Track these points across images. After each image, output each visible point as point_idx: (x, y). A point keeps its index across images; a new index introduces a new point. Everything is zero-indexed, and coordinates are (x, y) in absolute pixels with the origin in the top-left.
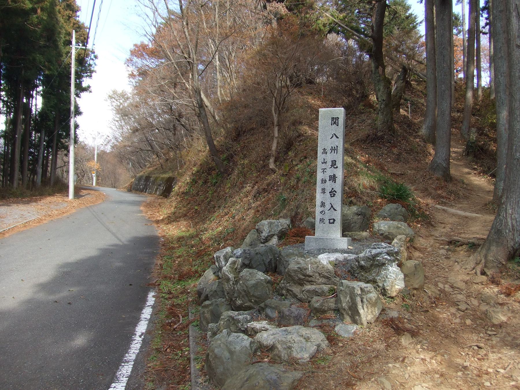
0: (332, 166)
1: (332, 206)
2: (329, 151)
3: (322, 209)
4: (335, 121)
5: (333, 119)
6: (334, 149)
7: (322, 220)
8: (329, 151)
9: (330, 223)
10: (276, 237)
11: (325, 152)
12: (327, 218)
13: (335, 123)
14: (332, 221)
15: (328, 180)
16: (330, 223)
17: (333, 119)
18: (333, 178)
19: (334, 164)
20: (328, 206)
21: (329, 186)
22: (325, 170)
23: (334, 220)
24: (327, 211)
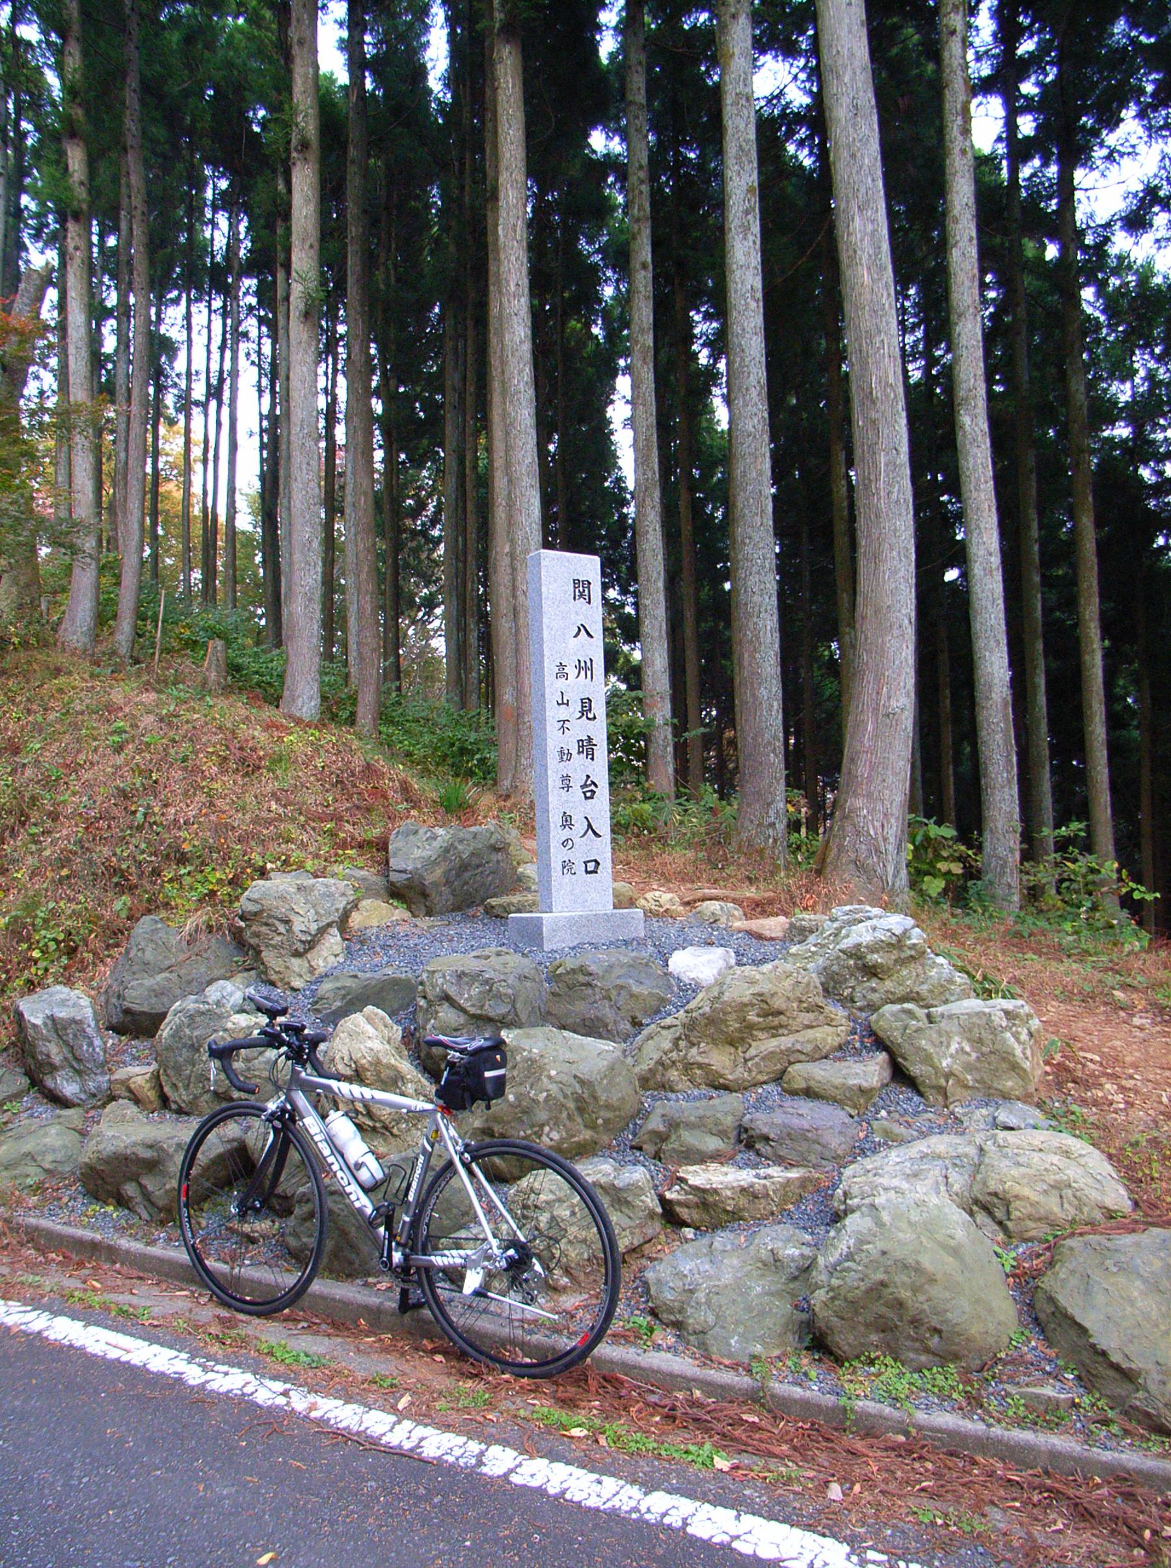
0: (582, 712)
1: (590, 826)
2: (572, 671)
3: (566, 833)
4: (581, 588)
5: (576, 582)
6: (584, 667)
7: (567, 866)
8: (572, 671)
9: (587, 872)
10: (334, 931)
11: (562, 674)
12: (578, 859)
13: (581, 595)
14: (591, 866)
15: (574, 752)
16: (587, 872)
17: (576, 582)
18: (587, 747)
19: (586, 706)
20: (580, 826)
21: (579, 767)
22: (567, 725)
23: (597, 863)
24: (577, 840)
